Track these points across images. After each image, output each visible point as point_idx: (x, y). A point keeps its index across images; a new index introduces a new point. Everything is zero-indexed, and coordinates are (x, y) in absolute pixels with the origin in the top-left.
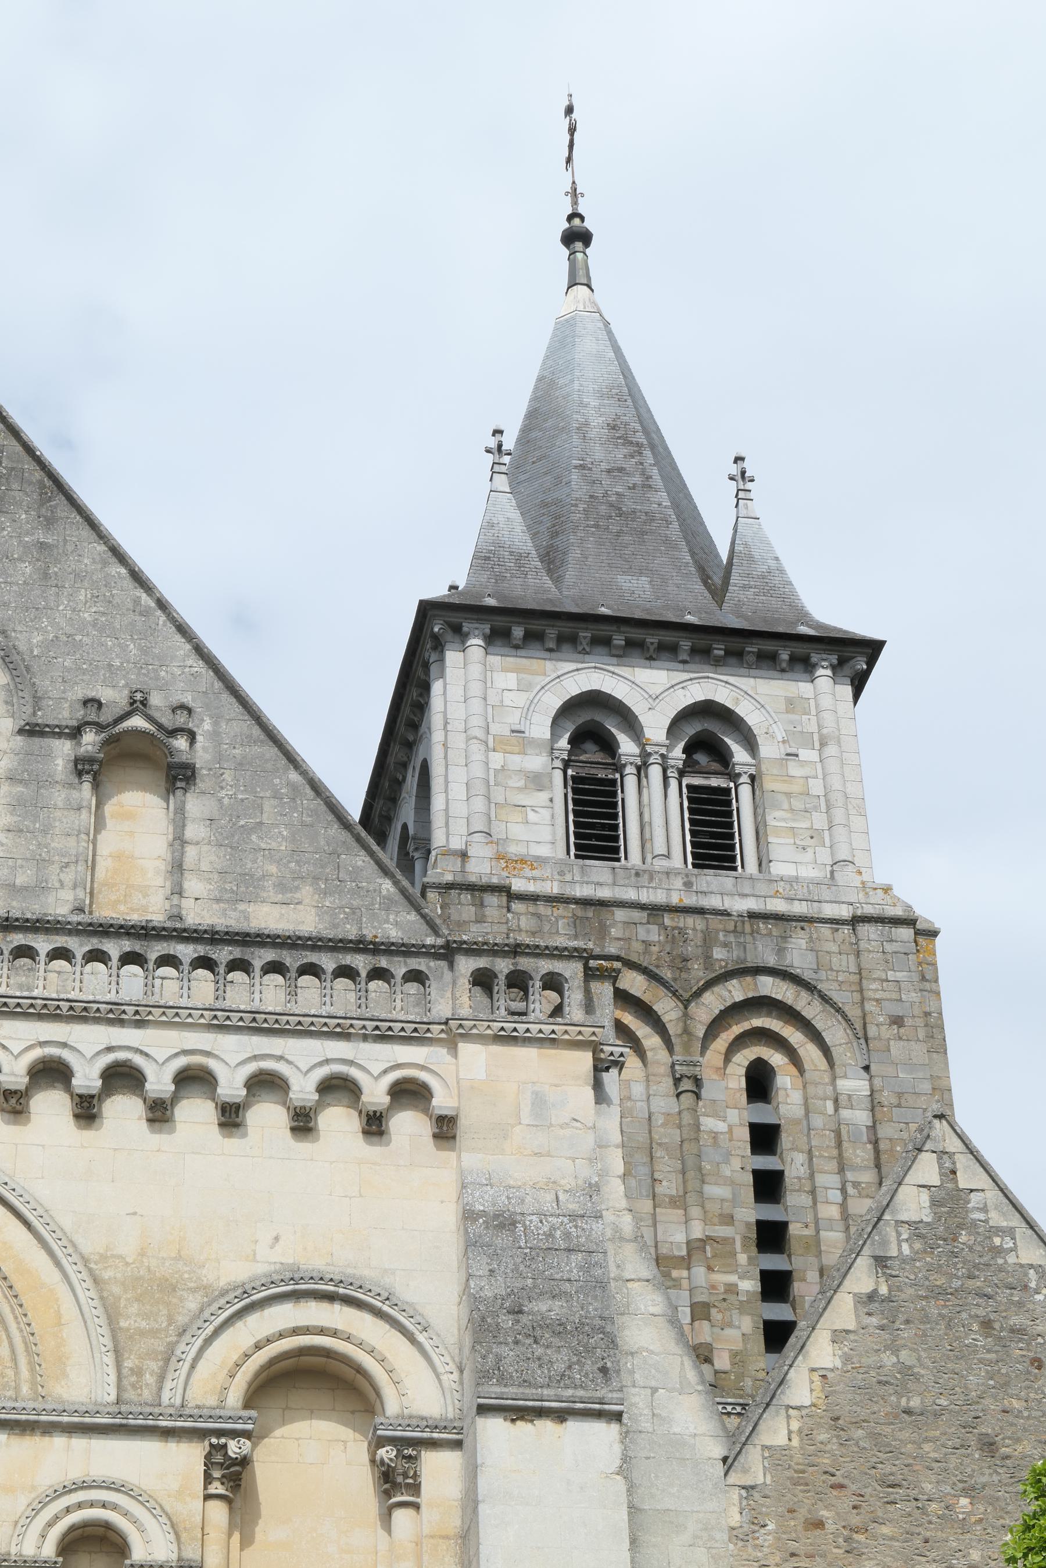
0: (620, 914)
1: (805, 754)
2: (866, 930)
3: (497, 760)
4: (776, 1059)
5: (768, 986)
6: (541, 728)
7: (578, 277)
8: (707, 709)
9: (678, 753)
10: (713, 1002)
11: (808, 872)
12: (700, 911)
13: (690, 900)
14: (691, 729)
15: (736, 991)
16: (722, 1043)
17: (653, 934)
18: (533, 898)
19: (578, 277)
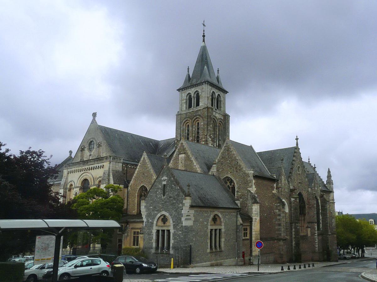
0: (188, 113)
1: (203, 93)
2: (204, 109)
3: (182, 102)
4: (199, 122)
5: (197, 117)
6: (185, 98)
7: (204, 41)
8: (197, 91)
9: (195, 96)
10: (194, 119)
11: (202, 105)
12: (193, 111)
13: (193, 110)
14: (196, 93)
15: (195, 118)
16: (195, 122)
17: (190, 114)
18: (183, 114)
19: (204, 41)
